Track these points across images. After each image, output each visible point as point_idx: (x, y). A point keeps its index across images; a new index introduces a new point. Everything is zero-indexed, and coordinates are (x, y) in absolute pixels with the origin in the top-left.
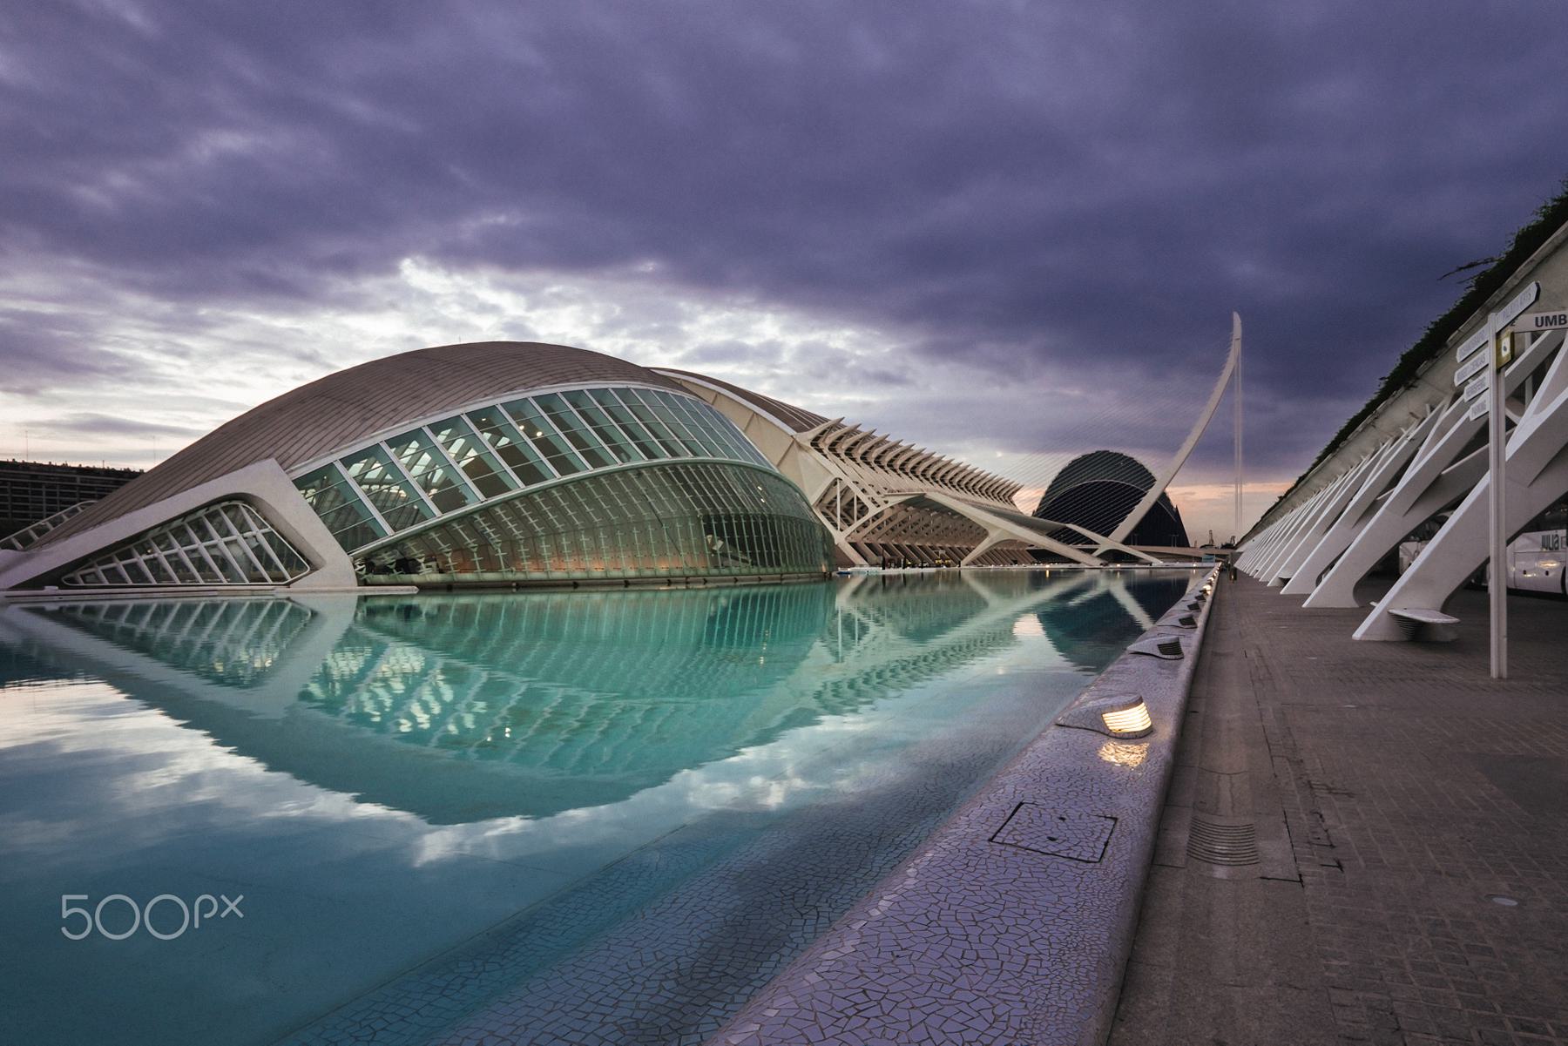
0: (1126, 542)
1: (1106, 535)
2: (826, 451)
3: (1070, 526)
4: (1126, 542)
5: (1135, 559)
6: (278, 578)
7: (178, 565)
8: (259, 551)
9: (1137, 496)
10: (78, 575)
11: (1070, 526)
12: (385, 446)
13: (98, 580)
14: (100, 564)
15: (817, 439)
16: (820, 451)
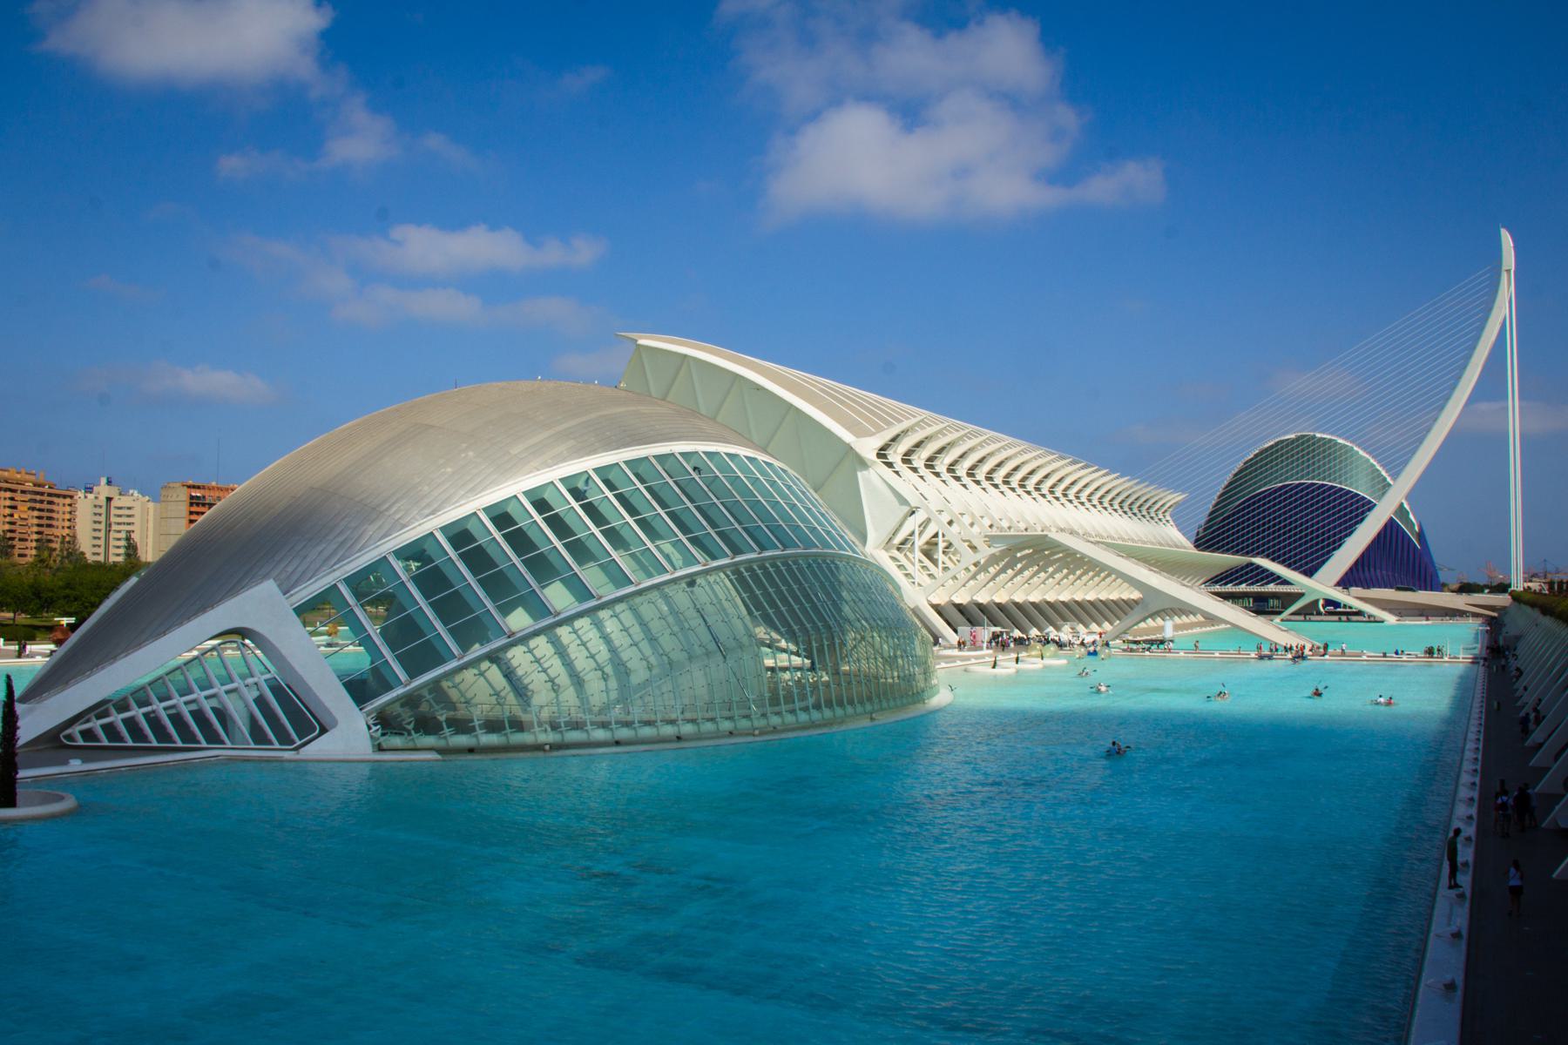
0: (1345, 582)
1: (1309, 573)
2: (899, 465)
3: (1259, 561)
4: (1345, 582)
5: (1351, 614)
6: (284, 739)
7: (177, 719)
8: (261, 701)
9: (1358, 509)
10: (76, 729)
11: (1259, 561)
12: (392, 560)
13: (96, 739)
14: (99, 717)
15: (882, 449)
16: (890, 465)
